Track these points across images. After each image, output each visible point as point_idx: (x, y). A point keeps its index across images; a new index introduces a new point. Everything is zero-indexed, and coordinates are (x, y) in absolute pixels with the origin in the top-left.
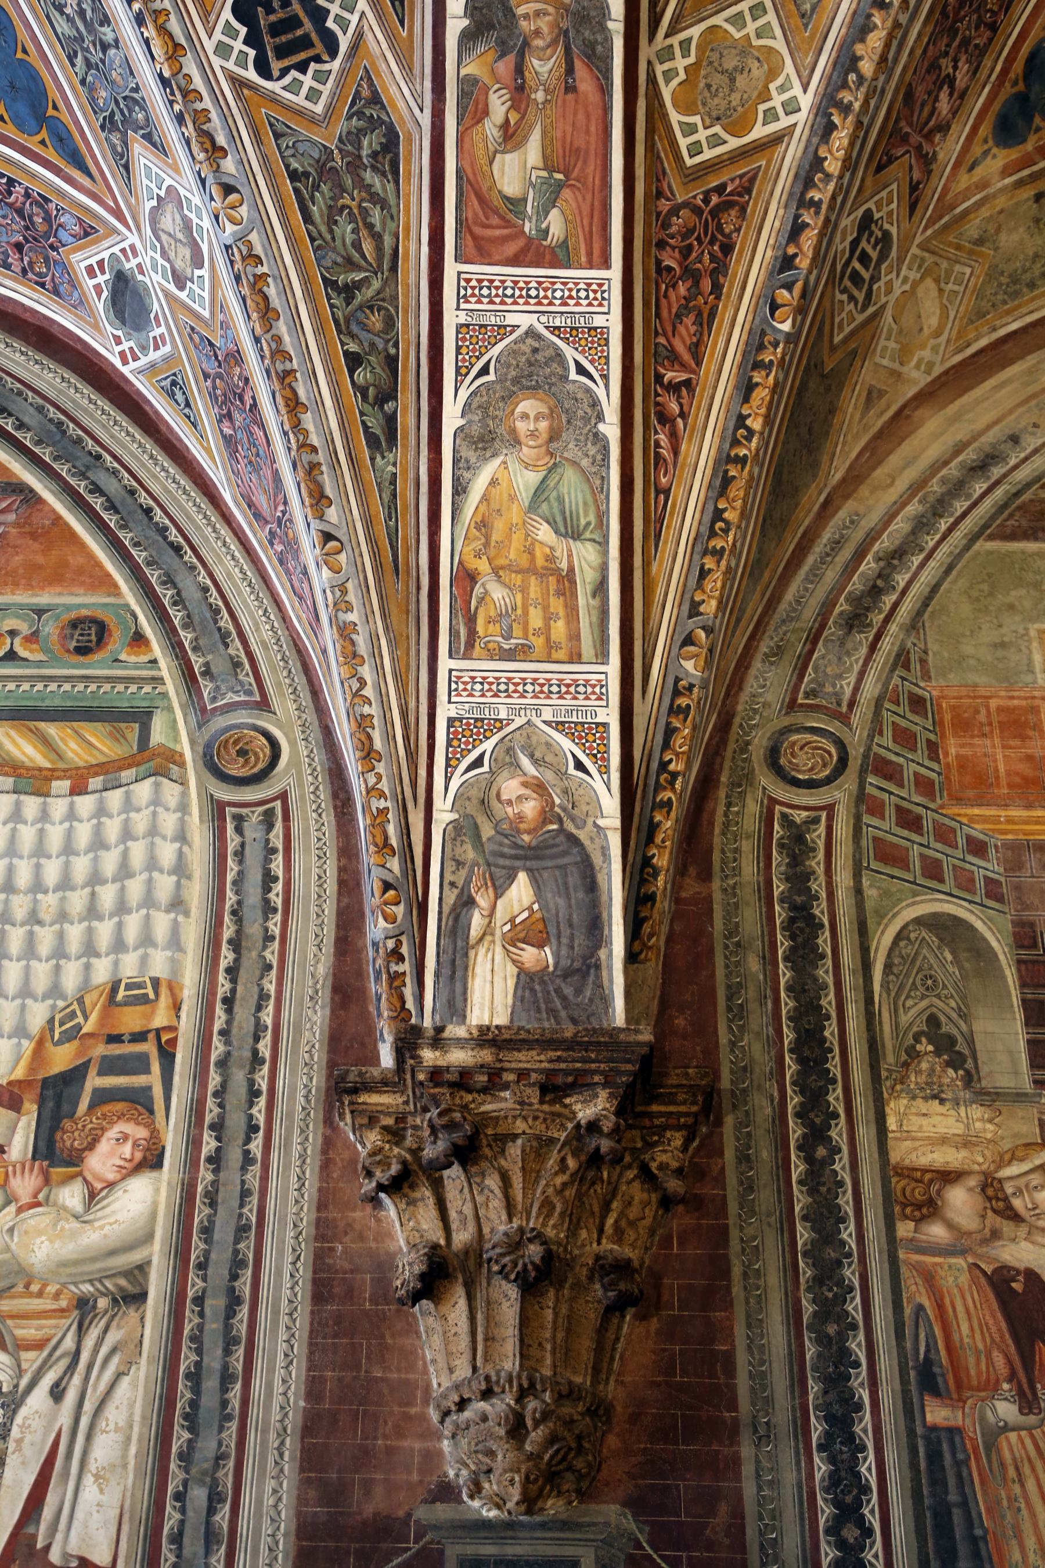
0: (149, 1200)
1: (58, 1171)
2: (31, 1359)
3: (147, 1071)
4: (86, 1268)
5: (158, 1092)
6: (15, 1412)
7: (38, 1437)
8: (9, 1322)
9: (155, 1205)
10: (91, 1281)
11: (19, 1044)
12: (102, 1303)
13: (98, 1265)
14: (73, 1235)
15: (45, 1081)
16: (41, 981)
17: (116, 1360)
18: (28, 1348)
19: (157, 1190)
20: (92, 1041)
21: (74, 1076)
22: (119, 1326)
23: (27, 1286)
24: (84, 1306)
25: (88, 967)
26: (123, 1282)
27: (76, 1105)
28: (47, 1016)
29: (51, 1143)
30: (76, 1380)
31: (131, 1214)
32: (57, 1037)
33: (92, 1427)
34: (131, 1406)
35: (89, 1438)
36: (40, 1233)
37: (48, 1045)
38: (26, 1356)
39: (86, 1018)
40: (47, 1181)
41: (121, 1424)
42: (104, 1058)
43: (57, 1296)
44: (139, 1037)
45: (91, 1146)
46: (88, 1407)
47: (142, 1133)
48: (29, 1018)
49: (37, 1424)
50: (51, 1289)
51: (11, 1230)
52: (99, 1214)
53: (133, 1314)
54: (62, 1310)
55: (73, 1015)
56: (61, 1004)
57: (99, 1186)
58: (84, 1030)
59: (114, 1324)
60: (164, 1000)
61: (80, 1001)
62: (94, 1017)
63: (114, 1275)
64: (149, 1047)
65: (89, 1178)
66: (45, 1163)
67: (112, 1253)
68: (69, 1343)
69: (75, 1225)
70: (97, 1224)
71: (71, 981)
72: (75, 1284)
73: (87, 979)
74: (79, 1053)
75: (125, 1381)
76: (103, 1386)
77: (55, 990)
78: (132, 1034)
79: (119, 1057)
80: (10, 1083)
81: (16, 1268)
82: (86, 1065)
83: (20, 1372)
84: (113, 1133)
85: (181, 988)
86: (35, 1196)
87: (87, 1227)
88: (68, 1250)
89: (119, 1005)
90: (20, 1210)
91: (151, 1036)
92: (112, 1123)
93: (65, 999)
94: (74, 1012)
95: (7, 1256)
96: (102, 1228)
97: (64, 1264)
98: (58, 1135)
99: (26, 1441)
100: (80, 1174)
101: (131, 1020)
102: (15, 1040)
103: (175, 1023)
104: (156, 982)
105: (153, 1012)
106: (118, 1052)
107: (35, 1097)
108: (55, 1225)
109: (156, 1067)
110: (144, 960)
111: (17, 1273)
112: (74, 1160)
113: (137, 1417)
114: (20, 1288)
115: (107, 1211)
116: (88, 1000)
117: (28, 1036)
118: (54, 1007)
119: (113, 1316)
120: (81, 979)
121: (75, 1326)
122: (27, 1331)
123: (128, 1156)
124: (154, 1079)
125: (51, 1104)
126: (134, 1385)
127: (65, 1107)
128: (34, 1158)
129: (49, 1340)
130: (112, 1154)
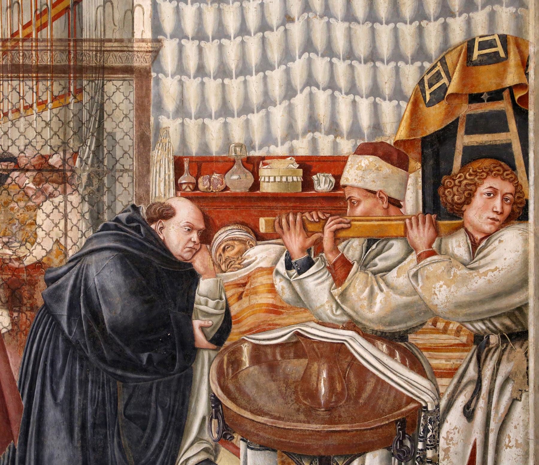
0: (521, 249)
1: (444, 223)
2: (446, 384)
3: (506, 129)
4: (478, 309)
5: (517, 148)
6: (440, 426)
7: (459, 448)
8: (425, 353)
9: (526, 253)
10: (482, 320)
11: (398, 106)
12: (494, 339)
13: (486, 307)
14: (465, 280)
15: (424, 139)
16: (408, 46)
17: (509, 388)
18: (443, 375)
19: (526, 240)
20: (456, 101)
21: (446, 135)
22: (509, 360)
23: (434, 324)
24: (479, 340)
25: (445, 27)
26: (508, 322)
27: (451, 162)
28: (417, 78)
29: (436, 197)
30: (482, 403)
31: (507, 262)
32: (428, 99)
33: (498, 442)
34: (526, 427)
35: (497, 451)
36: (438, 279)
37: (422, 105)
38: (442, 382)
39: (450, 79)
40: (437, 233)
41: (520, 441)
42: (469, 116)
43: (458, 332)
44: (496, 96)
45: (468, 201)
46: (494, 425)
47: (508, 188)
48: (403, 80)
49: (457, 437)
50: (453, 326)
51: (415, 275)
52: (482, 262)
53: (519, 351)
54: (464, 345)
55: (438, 76)
56: (427, 65)
57: (478, 236)
58: (449, 91)
59: (505, 357)
60: (513, 59)
61: (443, 61)
62: (456, 77)
63: (499, 316)
64: (504, 105)
65: (470, 229)
66: (434, 216)
67: (496, 296)
68: (472, 372)
69: (464, 271)
70: (481, 271)
71: (433, 44)
72: (470, 322)
73: (446, 39)
74: (449, 113)
75: (519, 406)
76: (502, 409)
77: (421, 53)
78: (490, 93)
79: (482, 115)
80: (396, 143)
81: (423, 308)
82: (455, 124)
83: (439, 396)
84: (484, 188)
85: (527, 46)
86: (430, 246)
87: (474, 273)
88: (462, 293)
89: (475, 65)
90: (420, 258)
91: (506, 94)
92: (483, 179)
93: (430, 61)
94: (438, 73)
95: (416, 298)
96: (485, 274)
97: (460, 305)
98: (441, 190)
99: (452, 450)
100: (462, 226)
101: (487, 79)
102: (395, 102)
103: (524, 81)
104: (504, 39)
105: (505, 71)
106: (480, 111)
107: (418, 156)
108: (449, 271)
109: (513, 125)
110: (492, 17)
111: (425, 312)
112: (456, 213)
113: (531, 436)
114: (429, 325)
115: (488, 259)
116: (449, 60)
117: (404, 98)
118: (422, 68)
119: (503, 351)
120: (441, 39)
121: (474, 359)
122: (439, 362)
123: (499, 209)
124: (512, 135)
125: (431, 162)
126: (526, 409)
127: (443, 165)
128: (424, 212)
129: (456, 369)
130: (485, 207)
